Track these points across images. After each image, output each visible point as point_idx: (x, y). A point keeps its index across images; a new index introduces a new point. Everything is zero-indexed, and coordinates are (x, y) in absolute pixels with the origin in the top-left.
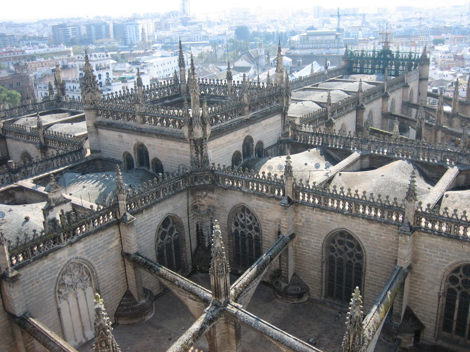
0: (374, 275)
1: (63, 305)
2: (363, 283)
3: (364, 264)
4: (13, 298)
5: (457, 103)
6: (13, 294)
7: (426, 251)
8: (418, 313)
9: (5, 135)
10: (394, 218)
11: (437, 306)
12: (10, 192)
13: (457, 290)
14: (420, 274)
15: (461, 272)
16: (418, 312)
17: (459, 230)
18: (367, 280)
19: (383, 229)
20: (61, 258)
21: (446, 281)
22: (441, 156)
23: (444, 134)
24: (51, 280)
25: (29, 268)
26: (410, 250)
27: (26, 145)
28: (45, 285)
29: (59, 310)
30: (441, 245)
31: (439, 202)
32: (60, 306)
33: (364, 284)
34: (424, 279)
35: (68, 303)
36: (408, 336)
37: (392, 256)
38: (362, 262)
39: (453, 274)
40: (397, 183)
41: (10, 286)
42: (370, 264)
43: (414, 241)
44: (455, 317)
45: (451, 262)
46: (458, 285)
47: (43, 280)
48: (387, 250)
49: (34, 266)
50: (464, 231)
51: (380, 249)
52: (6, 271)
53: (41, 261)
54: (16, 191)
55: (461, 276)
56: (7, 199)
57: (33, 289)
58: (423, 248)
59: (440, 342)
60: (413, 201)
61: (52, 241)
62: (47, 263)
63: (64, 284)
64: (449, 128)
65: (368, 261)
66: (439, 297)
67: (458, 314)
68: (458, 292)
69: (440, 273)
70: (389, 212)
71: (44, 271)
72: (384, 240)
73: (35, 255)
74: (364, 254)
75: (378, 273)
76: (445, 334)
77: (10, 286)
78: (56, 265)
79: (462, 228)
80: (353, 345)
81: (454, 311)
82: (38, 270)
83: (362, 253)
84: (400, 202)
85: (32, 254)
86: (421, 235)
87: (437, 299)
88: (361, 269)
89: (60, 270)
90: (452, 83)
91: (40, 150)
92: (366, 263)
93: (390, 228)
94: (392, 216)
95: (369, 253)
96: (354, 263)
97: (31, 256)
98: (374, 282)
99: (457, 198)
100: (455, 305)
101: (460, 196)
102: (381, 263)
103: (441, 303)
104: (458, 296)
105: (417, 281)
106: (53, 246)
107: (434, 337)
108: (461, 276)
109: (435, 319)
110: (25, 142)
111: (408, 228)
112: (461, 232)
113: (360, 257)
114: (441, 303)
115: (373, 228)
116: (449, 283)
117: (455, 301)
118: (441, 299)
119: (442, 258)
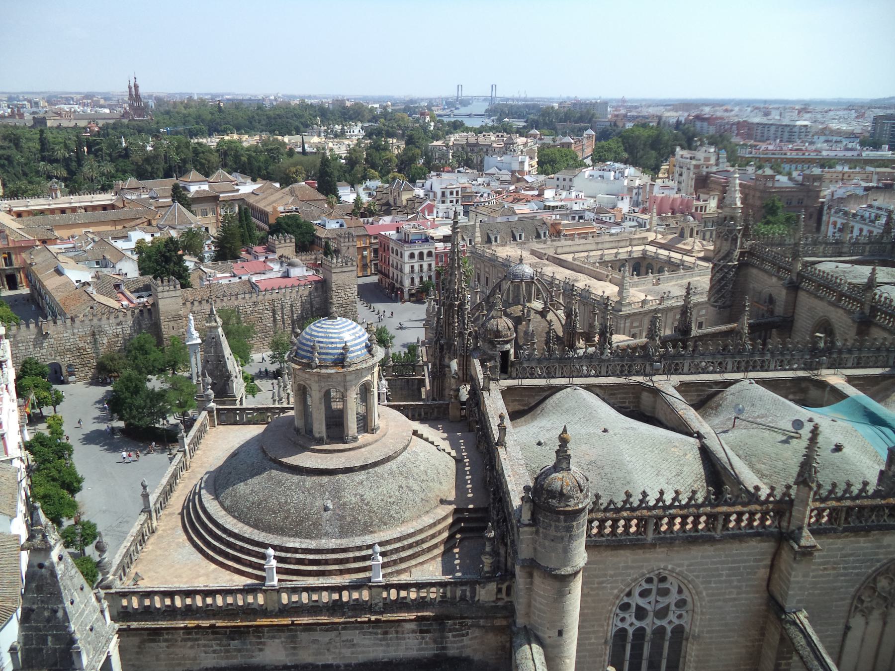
1: (857, 622)
4: (792, 579)
6: (793, 573)
9: (800, 283)
12: (803, 385)
20: (889, 546)
24: (857, 574)
25: (831, 540)
27: (832, 308)
28: (843, 578)
29: (848, 628)
32: (853, 623)
35: (867, 623)
41: (795, 558)
47: (845, 568)
49: (840, 541)
52: (797, 531)
53: (856, 536)
54: (814, 386)
56: (794, 393)
57: (822, 576)
61: (887, 511)
62: (862, 545)
63: (874, 589)
71: (851, 555)
73: (849, 523)
77: (795, 558)
78: (877, 554)
82: (843, 549)
85: (846, 519)
89: (878, 565)
91: (856, 326)
97: (842, 522)
106: (885, 521)
110: (831, 303)
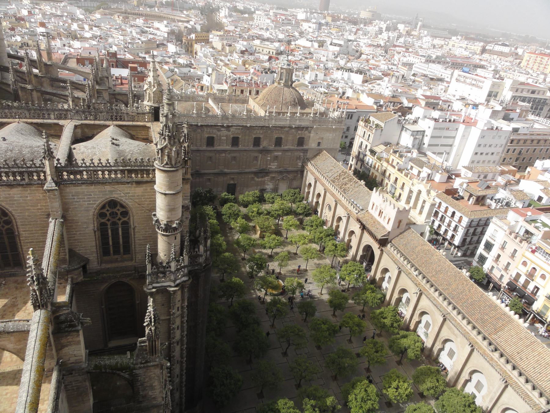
0: (28, 234)
2: (19, 244)
3: (15, 227)
5: (42, 65)
7: (74, 199)
8: (80, 250)
10: (35, 178)
11: (94, 239)
13: (107, 222)
14: (74, 220)
15: (107, 208)
16: (80, 250)
17: (98, 174)
18: (24, 240)
19: (27, 191)
21: (97, 218)
22: (54, 115)
23: (39, 94)
26: (60, 201)
30: (86, 191)
31: (70, 156)
33: (21, 246)
34: (78, 223)
36: (76, 272)
37: (43, 212)
38: (13, 226)
39: (102, 211)
40: (21, 146)
42: (22, 225)
43: (61, 193)
44: (111, 243)
45: (98, 202)
46: (107, 218)
48: (36, 208)
50: (102, 174)
51: (28, 209)
55: (108, 211)
58: (71, 197)
59: (104, 266)
60: (52, 159)
64: (43, 89)
65: (19, 224)
66: (95, 232)
67: (112, 240)
68: (109, 223)
69: (91, 213)
70: (28, 174)
72: (31, 200)
74: (13, 218)
75: (32, 231)
76: (106, 258)
79: (100, 173)
80: (41, 300)
81: (108, 238)
83: (10, 218)
84: (38, 162)
86: (66, 187)
87: (93, 234)
88: (13, 233)
90: (22, 44)
92: (17, 225)
93: (33, 188)
94: (33, 176)
95: (18, 216)
96: (4, 229)
98: (31, 239)
99: (83, 149)
100: (108, 234)
101: (85, 147)
102: (32, 222)
103: (97, 236)
104: (109, 226)
105: (72, 226)
107: (98, 264)
108: (108, 211)
109: (95, 250)
111: (54, 184)
112: (101, 176)
113: (9, 222)
114: (97, 236)
115: (16, 192)
116: (100, 219)
117: (107, 231)
118: (97, 233)
119: (90, 201)
